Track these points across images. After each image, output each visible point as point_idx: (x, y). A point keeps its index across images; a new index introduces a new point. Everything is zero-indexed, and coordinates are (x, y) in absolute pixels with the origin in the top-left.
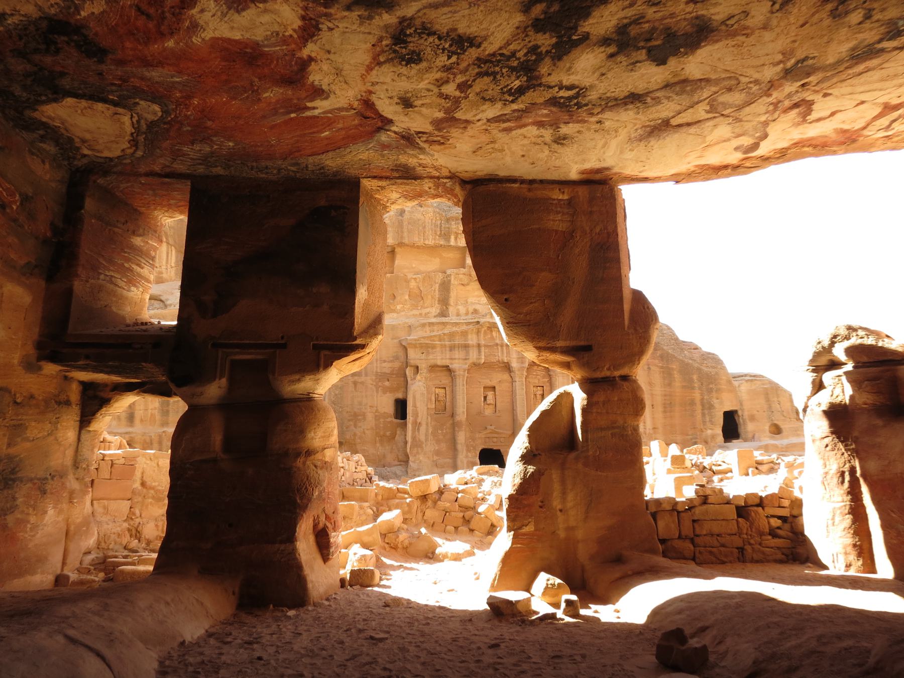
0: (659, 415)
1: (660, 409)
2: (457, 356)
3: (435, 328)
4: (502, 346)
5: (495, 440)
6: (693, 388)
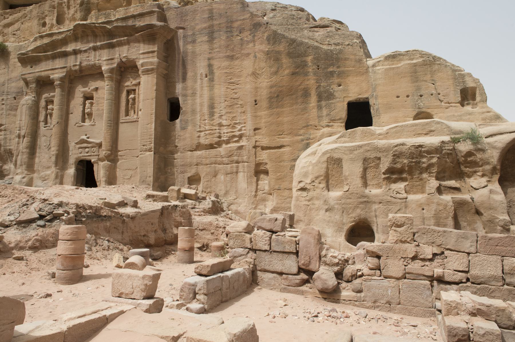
2: (57, 67)
5: (87, 150)
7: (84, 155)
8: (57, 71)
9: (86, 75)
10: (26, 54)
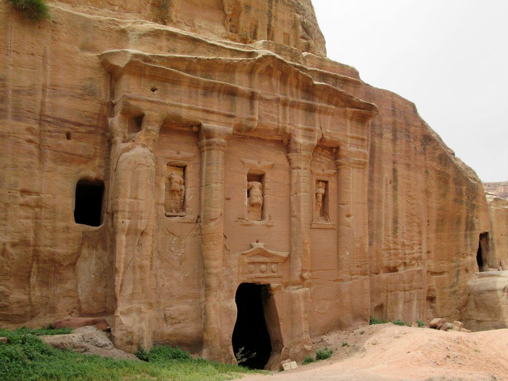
0: (432, 235)
1: (433, 226)
2: (216, 110)
3: (179, 45)
4: (285, 104)
5: (263, 267)
6: (461, 202)
7: (255, 276)
8: (215, 117)
9: (251, 138)
10: (150, 61)
